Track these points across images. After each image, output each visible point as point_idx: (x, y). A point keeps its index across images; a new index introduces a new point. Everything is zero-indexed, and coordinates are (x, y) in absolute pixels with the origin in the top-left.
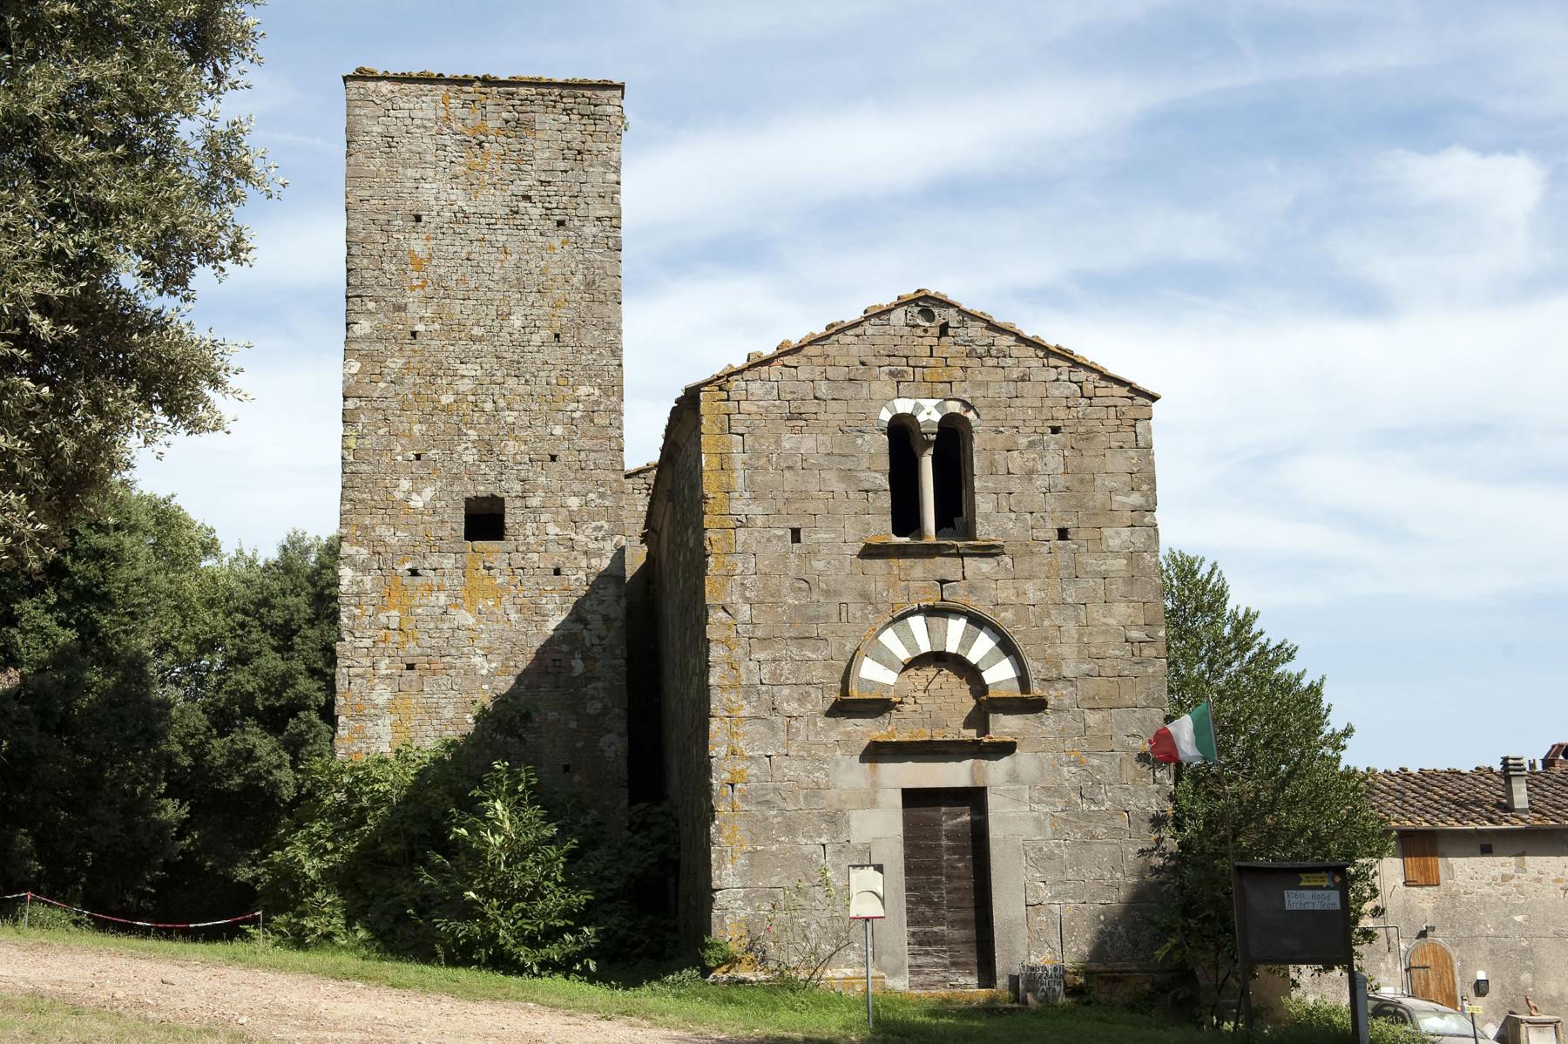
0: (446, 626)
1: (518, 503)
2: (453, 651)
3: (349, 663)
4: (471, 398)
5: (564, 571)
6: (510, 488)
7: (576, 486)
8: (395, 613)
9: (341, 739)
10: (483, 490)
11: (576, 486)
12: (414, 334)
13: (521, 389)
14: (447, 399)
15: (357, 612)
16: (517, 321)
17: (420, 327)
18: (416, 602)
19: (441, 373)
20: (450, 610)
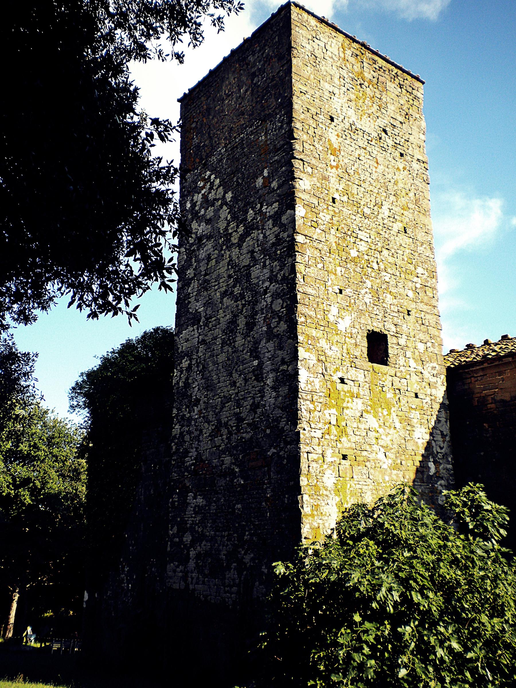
0: (362, 426)
1: (394, 340)
2: (368, 448)
3: (308, 449)
4: (366, 257)
5: (420, 396)
6: (387, 327)
7: (422, 336)
8: (333, 411)
9: (306, 515)
10: (377, 327)
11: (422, 336)
12: (334, 199)
13: (391, 260)
14: (354, 253)
15: (311, 406)
16: (385, 211)
17: (336, 196)
18: (345, 405)
19: (349, 233)
20: (364, 414)
